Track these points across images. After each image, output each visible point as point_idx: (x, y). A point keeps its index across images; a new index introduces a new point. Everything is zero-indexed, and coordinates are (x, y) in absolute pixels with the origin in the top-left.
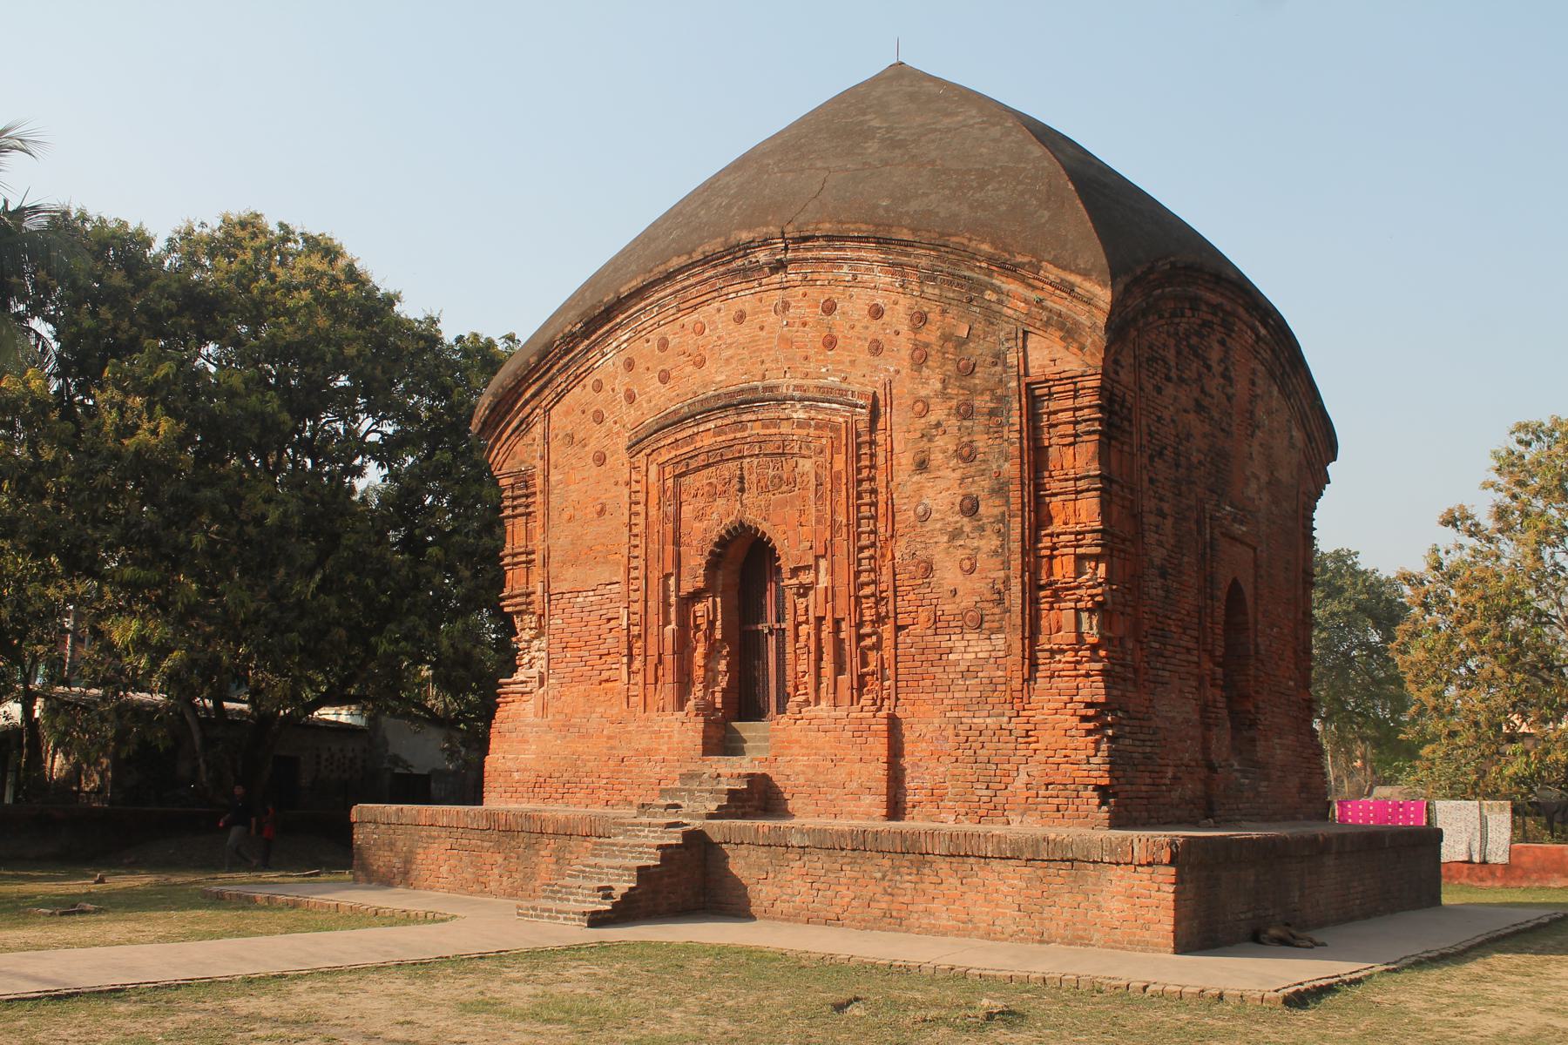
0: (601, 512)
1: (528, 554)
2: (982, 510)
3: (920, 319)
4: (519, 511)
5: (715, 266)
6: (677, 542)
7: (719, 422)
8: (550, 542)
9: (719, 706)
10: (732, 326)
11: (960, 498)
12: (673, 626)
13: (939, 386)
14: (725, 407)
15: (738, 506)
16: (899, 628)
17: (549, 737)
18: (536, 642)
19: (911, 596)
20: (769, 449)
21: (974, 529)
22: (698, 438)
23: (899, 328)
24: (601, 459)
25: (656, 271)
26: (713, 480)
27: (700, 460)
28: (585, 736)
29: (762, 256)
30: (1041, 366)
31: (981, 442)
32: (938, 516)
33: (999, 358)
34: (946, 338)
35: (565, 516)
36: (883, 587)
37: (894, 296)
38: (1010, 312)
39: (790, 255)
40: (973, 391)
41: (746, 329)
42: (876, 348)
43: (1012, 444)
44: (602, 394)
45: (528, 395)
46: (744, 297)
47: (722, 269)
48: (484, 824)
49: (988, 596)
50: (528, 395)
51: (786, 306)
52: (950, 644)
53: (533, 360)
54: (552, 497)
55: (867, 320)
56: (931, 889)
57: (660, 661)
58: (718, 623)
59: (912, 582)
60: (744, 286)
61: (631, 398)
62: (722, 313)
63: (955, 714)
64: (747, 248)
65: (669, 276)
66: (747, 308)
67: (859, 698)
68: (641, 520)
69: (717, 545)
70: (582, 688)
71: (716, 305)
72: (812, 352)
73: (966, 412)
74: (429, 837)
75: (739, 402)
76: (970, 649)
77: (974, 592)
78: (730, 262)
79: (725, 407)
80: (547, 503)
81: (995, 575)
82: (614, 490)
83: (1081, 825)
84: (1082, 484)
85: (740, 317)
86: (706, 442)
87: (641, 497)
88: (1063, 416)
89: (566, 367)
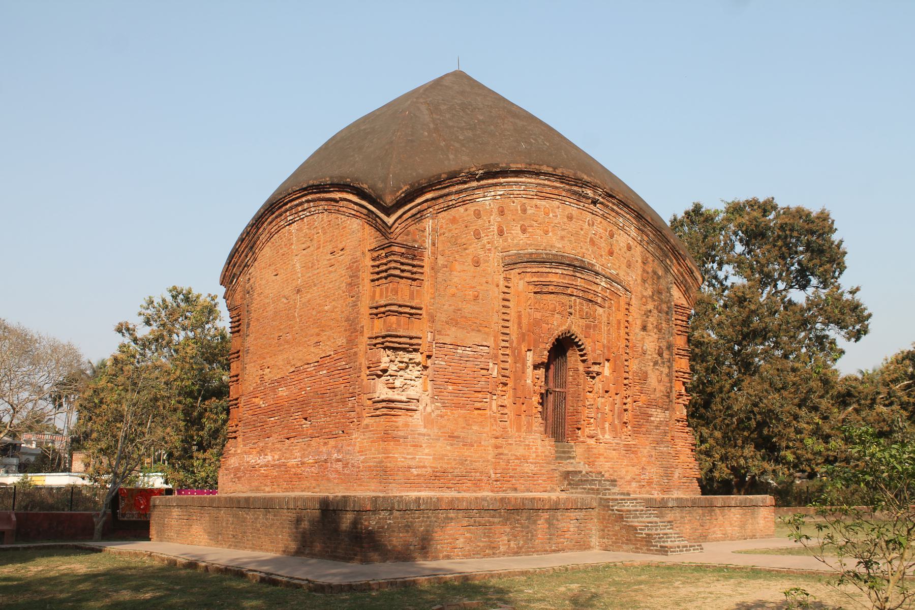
1: (412, 308)
4: (405, 274)
5: (562, 183)
7: (565, 272)
10: (566, 220)
14: (569, 265)
17: (439, 444)
24: (477, 264)
25: (533, 166)
27: (551, 289)
29: (590, 193)
39: (601, 200)
41: (572, 226)
44: (480, 222)
45: (429, 196)
46: (573, 210)
53: (444, 176)
61: (501, 233)
64: (585, 184)
65: (538, 174)
69: (557, 340)
71: (557, 203)
74: (447, 518)
75: (578, 267)
78: (572, 185)
84: (683, 352)
86: (555, 280)
88: (679, 322)
89: (460, 192)
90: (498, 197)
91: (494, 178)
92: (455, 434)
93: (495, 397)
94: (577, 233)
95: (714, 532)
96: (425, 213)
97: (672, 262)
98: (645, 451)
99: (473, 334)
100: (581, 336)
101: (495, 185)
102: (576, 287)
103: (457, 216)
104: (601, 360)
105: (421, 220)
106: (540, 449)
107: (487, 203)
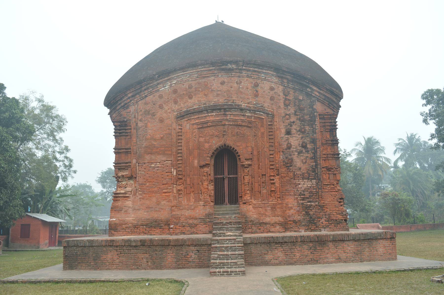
1: (126, 149)
2: (308, 146)
10: (220, 85)
11: (301, 143)
13: (293, 112)
14: (220, 109)
20: (236, 123)
31: (307, 128)
32: (294, 147)
33: (311, 106)
34: (296, 98)
39: (244, 68)
41: (225, 88)
42: (272, 99)
47: (218, 68)
48: (139, 244)
50: (130, 95)
51: (241, 82)
52: (299, 182)
56: (327, 251)
60: (225, 74)
63: (302, 202)
66: (226, 80)
69: (215, 151)
71: (213, 78)
73: (302, 120)
76: (305, 184)
78: (221, 66)
79: (220, 109)
83: (342, 230)
85: (223, 83)
88: (327, 124)
90: (174, 85)
91: (168, 76)
92: (151, 206)
93: (175, 186)
95: (326, 258)
100: (233, 147)
101: (169, 79)
105: (128, 107)
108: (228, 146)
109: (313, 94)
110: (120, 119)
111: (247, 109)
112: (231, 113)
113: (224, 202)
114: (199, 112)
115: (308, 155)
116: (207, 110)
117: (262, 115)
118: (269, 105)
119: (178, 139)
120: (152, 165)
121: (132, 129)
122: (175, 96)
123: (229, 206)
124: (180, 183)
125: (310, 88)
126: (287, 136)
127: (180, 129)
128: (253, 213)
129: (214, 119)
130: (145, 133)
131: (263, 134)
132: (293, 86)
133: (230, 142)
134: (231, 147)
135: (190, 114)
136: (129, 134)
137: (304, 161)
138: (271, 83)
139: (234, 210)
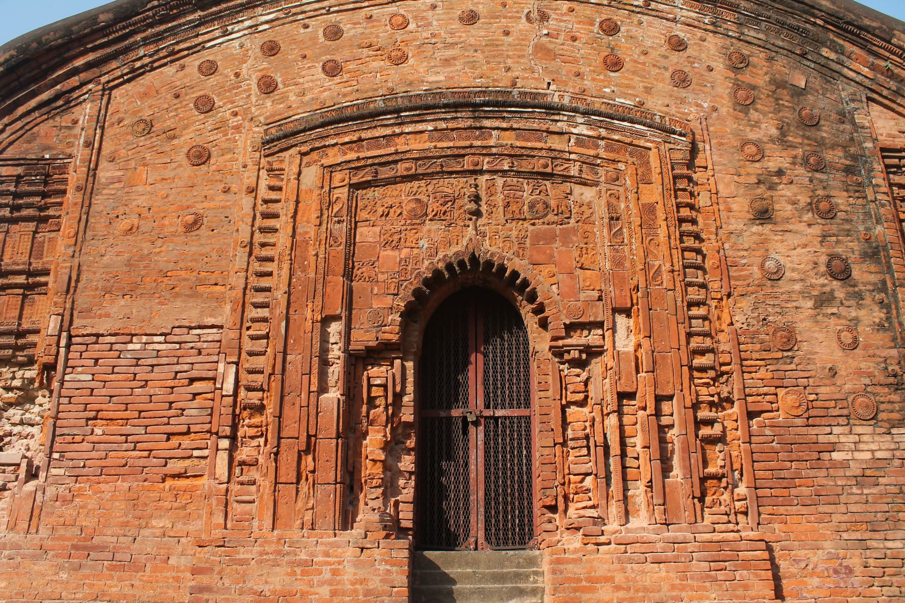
0: (194, 225)
1: (29, 274)
2: (855, 274)
3: (739, 64)
4: (25, 212)
6: (349, 274)
7: (444, 126)
8: (83, 259)
9: (409, 524)
10: (456, 25)
11: (824, 259)
12: (334, 395)
13: (774, 132)
14: (455, 107)
15: (471, 231)
16: (751, 415)
18: (15, 414)
19: (762, 373)
20: (526, 166)
21: (849, 296)
22: (401, 140)
23: (713, 64)
26: (425, 199)
27: (401, 169)
28: (134, 566)
30: (889, 135)
31: (841, 200)
32: (795, 275)
34: (779, 84)
35: (122, 225)
36: (725, 358)
37: (699, 33)
38: (851, 74)
40: (821, 143)
41: (476, 34)
42: (682, 80)
43: (883, 206)
44: (213, 80)
49: (882, 379)
52: (832, 439)
54: (98, 200)
55: (664, 50)
57: (309, 448)
58: (407, 399)
59: (765, 355)
61: (268, 86)
62: (439, 11)
63: (858, 535)
67: (702, 511)
68: (282, 239)
69: (426, 282)
70: (123, 485)
72: (585, 69)
77: (859, 373)
79: (455, 107)
80: (87, 206)
81: (886, 353)
82: (221, 199)
87: (285, 209)
90: (266, 26)
92: (97, 540)
94: (493, 44)
96: (75, 95)
97: (841, 51)
98: (817, 558)
99: (178, 303)
102: (486, 151)
103: (157, 84)
104: (599, 313)
105: (68, 106)
106: (349, 573)
107: (236, 43)
108: (489, 264)
109: (845, 71)
110: (27, 151)
111: (575, 110)
112: (504, 125)
113: (467, 536)
114: (362, 117)
115: (862, 313)
116: (398, 111)
117: (642, 135)
118: (667, 101)
119: (263, 230)
120: (130, 347)
121: (70, 195)
122: (265, 65)
123: (487, 553)
124: (252, 432)
125: (834, 48)
126: (755, 229)
127: (272, 188)
128: (618, 588)
129: (428, 145)
130: (121, 210)
131: (650, 209)
132: (761, 36)
133: (497, 240)
134: (502, 268)
135: (323, 125)
136: (51, 212)
137: (847, 338)
138: (669, 24)
139: (517, 576)
